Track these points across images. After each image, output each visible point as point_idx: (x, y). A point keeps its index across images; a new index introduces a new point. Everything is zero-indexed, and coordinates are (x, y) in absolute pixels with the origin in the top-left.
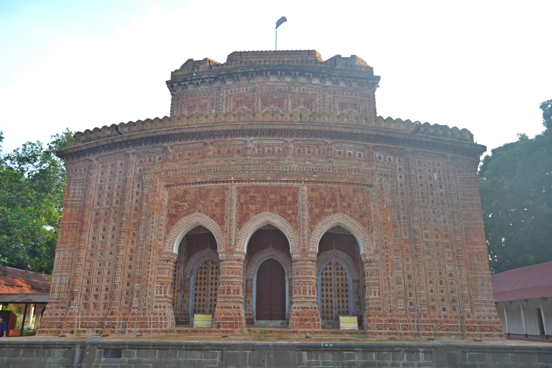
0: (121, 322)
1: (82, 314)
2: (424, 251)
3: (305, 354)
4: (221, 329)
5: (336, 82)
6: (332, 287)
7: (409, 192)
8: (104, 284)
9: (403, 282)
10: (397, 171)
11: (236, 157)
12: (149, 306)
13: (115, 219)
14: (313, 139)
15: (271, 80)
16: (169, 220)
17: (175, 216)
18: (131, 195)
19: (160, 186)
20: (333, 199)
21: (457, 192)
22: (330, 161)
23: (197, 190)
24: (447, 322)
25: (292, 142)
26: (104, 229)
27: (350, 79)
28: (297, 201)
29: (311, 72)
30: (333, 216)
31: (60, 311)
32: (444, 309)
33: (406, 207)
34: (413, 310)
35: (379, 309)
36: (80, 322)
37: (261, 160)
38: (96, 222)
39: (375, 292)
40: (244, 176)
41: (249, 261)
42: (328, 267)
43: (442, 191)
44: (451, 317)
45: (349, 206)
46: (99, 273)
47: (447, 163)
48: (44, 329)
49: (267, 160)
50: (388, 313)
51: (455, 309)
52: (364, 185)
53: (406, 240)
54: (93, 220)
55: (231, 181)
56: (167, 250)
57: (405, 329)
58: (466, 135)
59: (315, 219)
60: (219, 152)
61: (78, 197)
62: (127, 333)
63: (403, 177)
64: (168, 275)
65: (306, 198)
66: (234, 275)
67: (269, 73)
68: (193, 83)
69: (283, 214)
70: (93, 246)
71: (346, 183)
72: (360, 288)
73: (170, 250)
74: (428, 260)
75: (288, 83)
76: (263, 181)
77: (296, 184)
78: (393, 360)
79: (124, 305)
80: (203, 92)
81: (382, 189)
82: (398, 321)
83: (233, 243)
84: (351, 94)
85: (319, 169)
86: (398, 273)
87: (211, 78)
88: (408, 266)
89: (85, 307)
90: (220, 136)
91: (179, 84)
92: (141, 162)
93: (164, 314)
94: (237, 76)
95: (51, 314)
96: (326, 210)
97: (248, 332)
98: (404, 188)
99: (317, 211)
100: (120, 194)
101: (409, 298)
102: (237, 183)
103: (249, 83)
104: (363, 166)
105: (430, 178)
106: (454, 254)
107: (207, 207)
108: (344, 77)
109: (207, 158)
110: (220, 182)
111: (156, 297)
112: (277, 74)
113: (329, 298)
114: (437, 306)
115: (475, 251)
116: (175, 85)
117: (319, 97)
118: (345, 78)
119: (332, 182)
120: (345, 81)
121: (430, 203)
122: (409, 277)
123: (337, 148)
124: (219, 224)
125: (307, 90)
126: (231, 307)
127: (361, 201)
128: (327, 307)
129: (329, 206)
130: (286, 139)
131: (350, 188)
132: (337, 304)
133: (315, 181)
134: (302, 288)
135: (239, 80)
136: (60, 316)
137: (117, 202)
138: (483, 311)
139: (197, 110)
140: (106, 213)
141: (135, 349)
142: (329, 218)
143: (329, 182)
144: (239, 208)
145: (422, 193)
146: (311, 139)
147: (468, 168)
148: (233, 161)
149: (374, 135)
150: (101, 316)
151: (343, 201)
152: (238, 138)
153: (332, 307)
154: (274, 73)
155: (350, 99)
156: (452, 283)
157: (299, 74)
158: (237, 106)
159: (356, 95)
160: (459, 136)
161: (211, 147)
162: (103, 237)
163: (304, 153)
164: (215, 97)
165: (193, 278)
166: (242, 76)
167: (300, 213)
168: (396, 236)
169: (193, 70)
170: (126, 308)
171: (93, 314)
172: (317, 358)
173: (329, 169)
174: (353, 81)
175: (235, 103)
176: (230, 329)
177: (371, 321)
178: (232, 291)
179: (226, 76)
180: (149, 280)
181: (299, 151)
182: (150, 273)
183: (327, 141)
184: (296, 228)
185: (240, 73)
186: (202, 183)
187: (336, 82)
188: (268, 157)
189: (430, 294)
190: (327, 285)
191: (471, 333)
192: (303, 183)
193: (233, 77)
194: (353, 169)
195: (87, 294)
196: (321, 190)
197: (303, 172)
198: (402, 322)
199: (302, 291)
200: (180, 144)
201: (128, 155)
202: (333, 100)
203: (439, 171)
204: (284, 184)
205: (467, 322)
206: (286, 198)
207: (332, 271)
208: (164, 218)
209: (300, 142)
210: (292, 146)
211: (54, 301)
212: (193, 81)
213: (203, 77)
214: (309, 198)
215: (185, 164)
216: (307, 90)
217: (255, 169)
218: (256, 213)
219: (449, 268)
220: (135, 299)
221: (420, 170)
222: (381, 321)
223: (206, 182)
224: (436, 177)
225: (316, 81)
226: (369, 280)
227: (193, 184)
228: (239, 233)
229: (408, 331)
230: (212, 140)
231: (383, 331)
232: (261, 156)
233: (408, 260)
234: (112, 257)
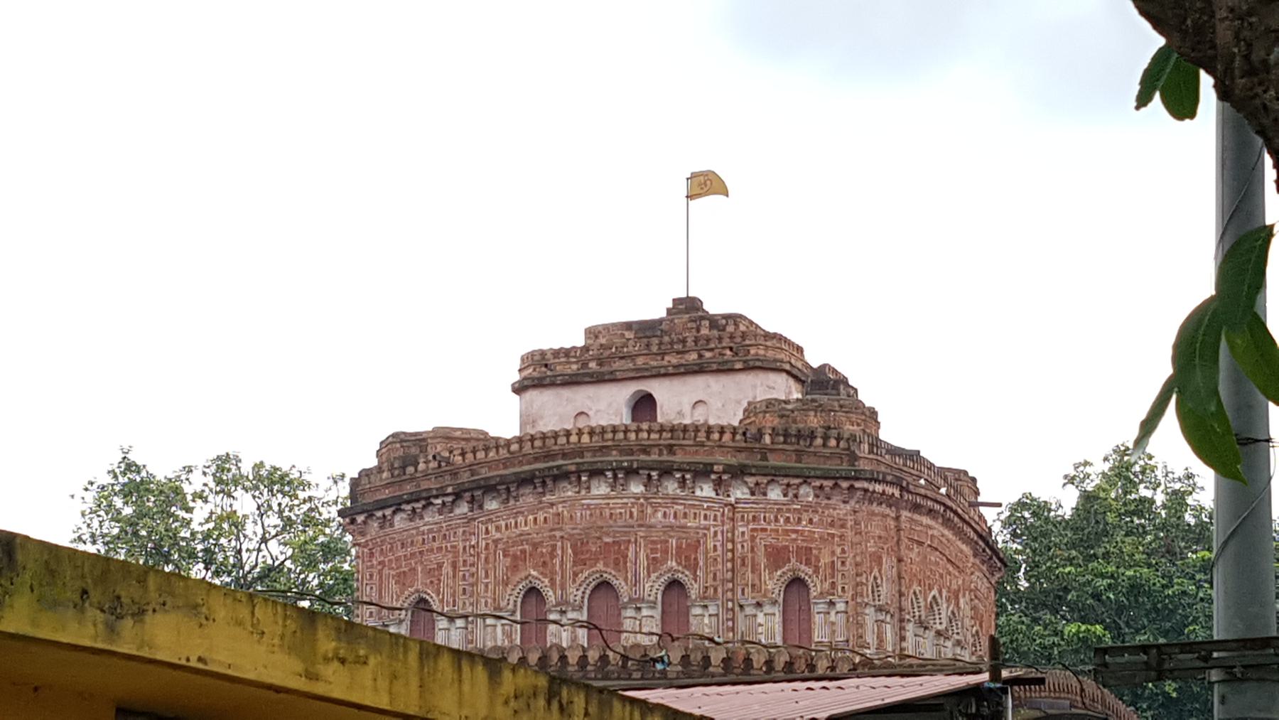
15: (594, 492)
67: (584, 479)
103: (541, 502)
116: (360, 519)
117: (716, 533)
135: (516, 499)
139: (419, 582)
154: (596, 473)
155: (794, 536)
157: (660, 476)
158: (514, 568)
159: (811, 521)
169: (404, 468)
174: (799, 486)
179: (479, 493)
193: (498, 491)
202: (753, 538)
225: (706, 490)
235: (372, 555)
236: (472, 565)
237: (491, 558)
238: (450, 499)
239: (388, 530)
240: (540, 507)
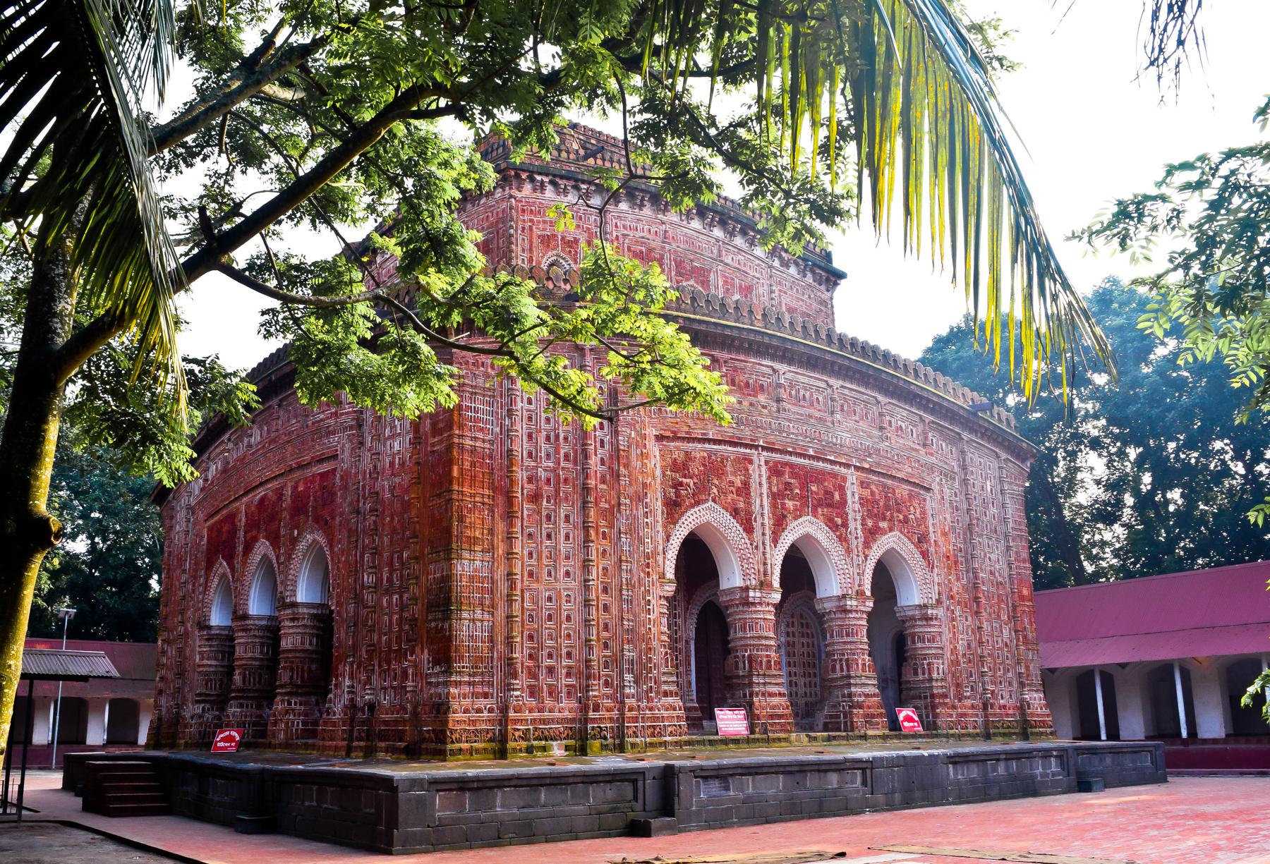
31: (481, 703)
40: (778, 440)
48: (457, 746)
55: (756, 447)
61: (481, 429)
69: (830, 523)
75: (718, 241)
89: (532, 695)
95: (466, 711)
110: (742, 445)
130: (832, 381)
137: (567, 456)
141: (750, 774)
149: (935, 403)
150: (567, 714)
152: (765, 362)
167: (852, 525)
176: (783, 735)
183: (880, 398)
211: (466, 679)
218: (796, 518)
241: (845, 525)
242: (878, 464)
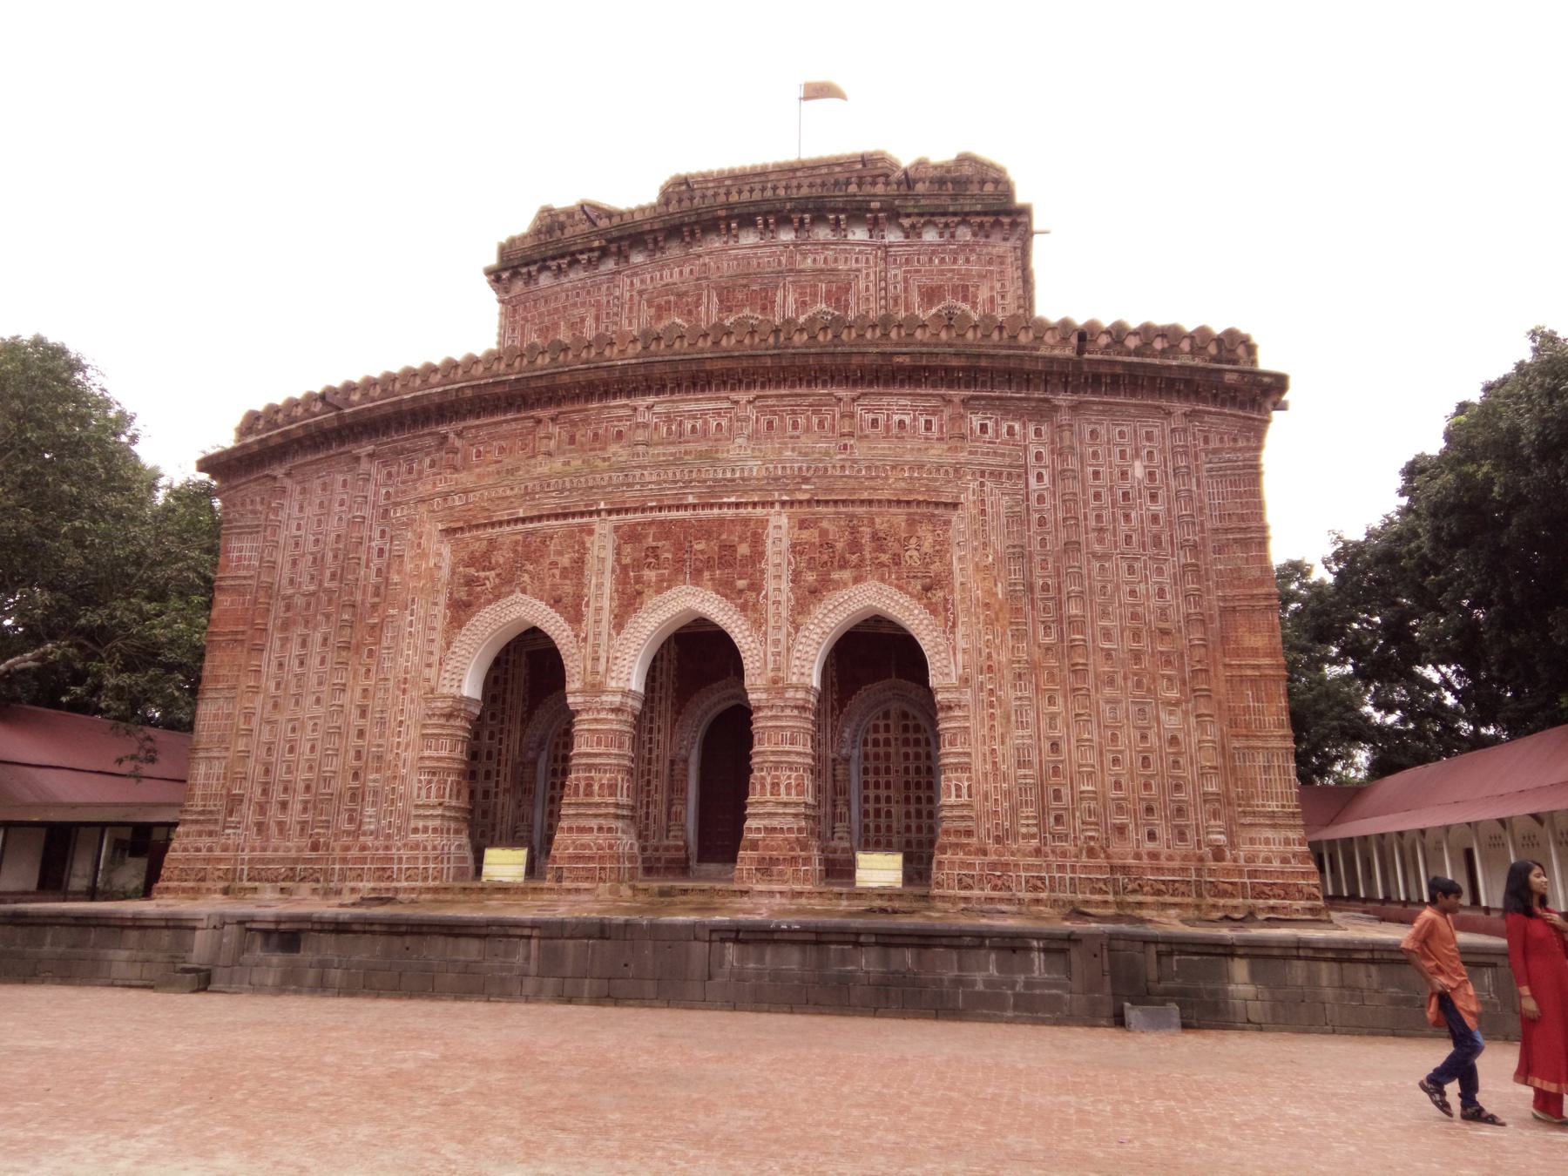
0: (337, 867)
1: (253, 849)
2: (1097, 676)
3: (731, 951)
4: (567, 884)
5: (912, 232)
6: (892, 777)
7: (1060, 515)
8: (302, 776)
9: (1036, 760)
10: (1031, 460)
11: (613, 448)
12: (399, 829)
13: (328, 616)
14: (804, 390)
16: (452, 617)
17: (468, 605)
18: (364, 558)
19: (430, 534)
20: (855, 546)
21: (1201, 509)
22: (845, 447)
23: (519, 537)
24: (1159, 870)
25: (749, 402)
26: (304, 644)
27: (950, 219)
28: (762, 554)
29: (843, 211)
30: (853, 589)
31: (206, 841)
32: (1152, 836)
33: (1050, 560)
34: (1063, 837)
35: (969, 833)
36: (246, 867)
37: (672, 454)
38: (286, 626)
39: (958, 788)
40: (630, 497)
41: (679, 713)
42: (882, 723)
43: (1159, 508)
44: (1170, 858)
45: (897, 560)
46: (291, 750)
47: (1173, 431)
49: (686, 453)
50: (991, 845)
51: (1182, 836)
52: (937, 504)
53: (1048, 649)
54: (279, 622)
55: (598, 512)
56: (445, 691)
57: (1035, 888)
58: (1235, 346)
59: (808, 596)
60: (572, 440)
61: (248, 568)
62: (346, 891)
63: (1046, 478)
64: (449, 751)
65: (785, 544)
66: (602, 749)
67: (734, 225)
68: (549, 268)
69: (726, 589)
70: (278, 685)
71: (889, 502)
72: (922, 780)
73: (454, 690)
74: (1108, 702)
75: (786, 246)
76: (678, 508)
77: (759, 511)
78: (961, 969)
79: (347, 827)
80: (575, 288)
81: (983, 512)
82: (1016, 865)
83: (602, 668)
84: (955, 261)
85: (817, 469)
86: (1018, 736)
87: (592, 250)
88: (1053, 717)
89: (259, 831)
90: (575, 398)
91: (515, 274)
92: (390, 475)
93: (434, 848)
94: (656, 241)
95: (185, 850)
96: (835, 576)
97: (629, 893)
98: (1047, 505)
99: (811, 577)
100: (341, 557)
101: (1054, 804)
102: (614, 517)
104: (937, 453)
105: (1124, 474)
106: (1184, 683)
107: (542, 581)
108: (933, 215)
109: (540, 458)
110: (574, 515)
111: (417, 806)
112: (755, 224)
113: (883, 805)
114: (1132, 827)
115: (1249, 672)
116: (505, 275)
118: (936, 219)
119: (853, 502)
120: (936, 225)
121: (1121, 543)
122: (1055, 746)
123: (869, 411)
124: (569, 620)
125: (836, 260)
126: (591, 829)
127: (927, 547)
128: (878, 828)
129: (844, 565)
130: (734, 396)
131: (899, 516)
132: (904, 821)
133: (809, 502)
134: (769, 780)
135: (662, 250)
136: (204, 853)
137: (333, 575)
138: (1267, 842)
140: (309, 604)
142: (840, 595)
143: (844, 502)
144: (617, 579)
145: (1099, 517)
146: (798, 390)
147: (1235, 440)
148: (604, 460)
149: (963, 369)
150: (293, 854)
151: (881, 549)
152: (618, 402)
153: (889, 828)
154: (747, 221)
156: (1176, 763)
157: (813, 222)
158: (659, 318)
159: (967, 261)
160: (1213, 349)
161: (555, 429)
162: (302, 663)
163: (784, 429)
164: (604, 300)
165: (544, 755)
166: (666, 239)
167: (770, 585)
168: (1019, 636)
170: (349, 833)
171: (276, 850)
172: (761, 959)
173: (843, 467)
174: (958, 224)
175: (653, 311)
177: (948, 865)
178: (596, 787)
180: (400, 764)
181: (770, 423)
182: (402, 747)
183: (841, 392)
184: (758, 624)
185: (660, 230)
186: (531, 519)
187: (912, 232)
188: (690, 446)
189: (1113, 794)
190: (877, 771)
191: (1222, 902)
192: (777, 506)
194: (906, 462)
195: (263, 799)
196: (825, 524)
197: (776, 479)
198: (1027, 868)
199: (768, 787)
200: (477, 426)
201: (357, 459)
202: (906, 280)
203: (1150, 453)
204: (729, 513)
205: (1212, 872)
206: (733, 548)
207: (891, 736)
208: (441, 611)
209: (770, 402)
210: (751, 412)
212: (550, 263)
213: (573, 248)
214: (794, 546)
215: (489, 474)
216: (836, 260)
217: (654, 478)
218: (659, 592)
219: (1171, 722)
220: (369, 811)
221: (1095, 454)
222: (971, 865)
223: (540, 518)
224: (1138, 470)
225: (859, 234)
226: (949, 753)
227: (508, 522)
228: (616, 642)
229: (1043, 895)
230: (552, 411)
231: (976, 893)
232: (672, 443)
233: (1051, 701)
234: (319, 711)
235: (515, 311)
236: (616, 314)
237: (635, 308)
238: (596, 254)
239: (532, 288)
240: (687, 258)
241: (756, 587)
242: (830, 490)
